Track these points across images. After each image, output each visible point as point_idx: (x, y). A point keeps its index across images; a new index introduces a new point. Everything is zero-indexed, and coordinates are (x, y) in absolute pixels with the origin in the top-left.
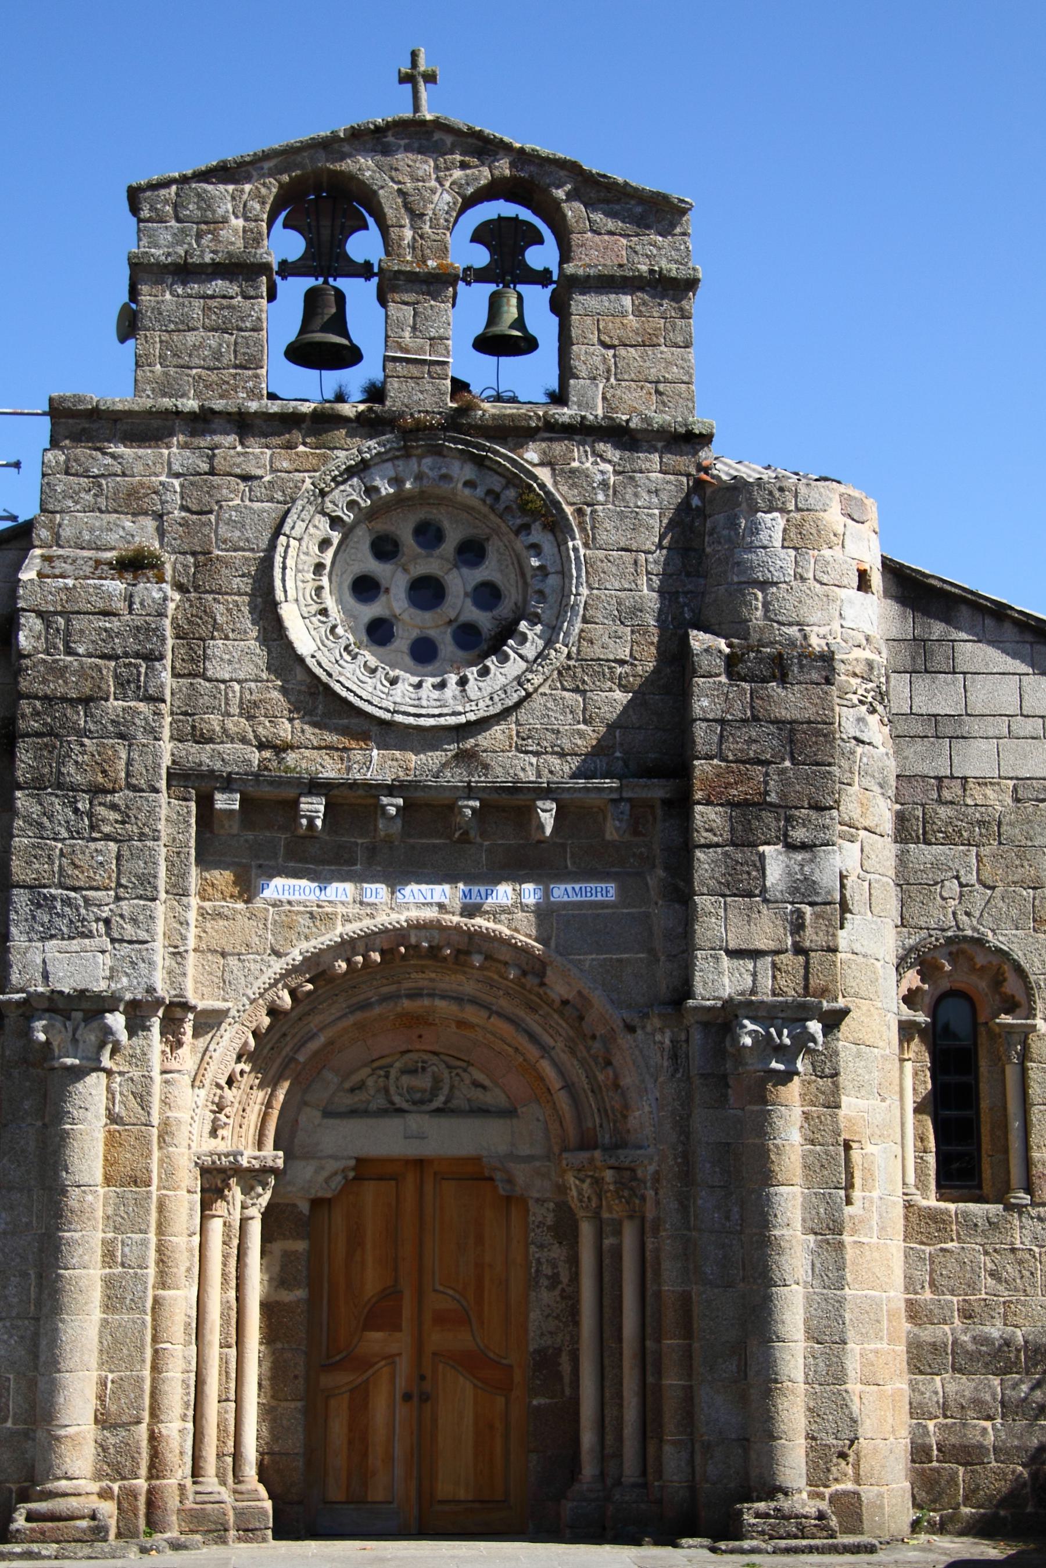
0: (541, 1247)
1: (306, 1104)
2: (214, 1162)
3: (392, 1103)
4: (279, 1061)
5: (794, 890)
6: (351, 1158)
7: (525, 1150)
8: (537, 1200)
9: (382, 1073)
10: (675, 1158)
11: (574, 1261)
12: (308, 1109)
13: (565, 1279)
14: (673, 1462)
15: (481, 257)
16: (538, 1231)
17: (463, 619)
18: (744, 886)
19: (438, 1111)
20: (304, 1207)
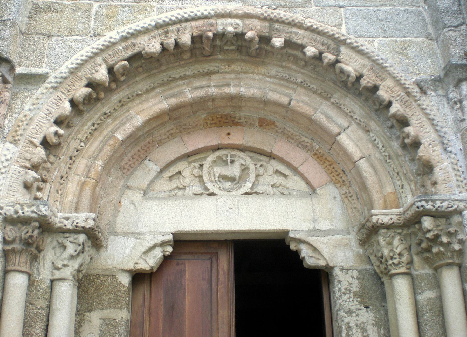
0: (350, 312)
1: (128, 187)
2: (16, 212)
3: (207, 189)
4: (101, 138)
6: (166, 234)
7: (325, 225)
8: (342, 269)
9: (197, 165)
12: (129, 193)
16: (345, 297)
19: (246, 194)
20: (125, 280)
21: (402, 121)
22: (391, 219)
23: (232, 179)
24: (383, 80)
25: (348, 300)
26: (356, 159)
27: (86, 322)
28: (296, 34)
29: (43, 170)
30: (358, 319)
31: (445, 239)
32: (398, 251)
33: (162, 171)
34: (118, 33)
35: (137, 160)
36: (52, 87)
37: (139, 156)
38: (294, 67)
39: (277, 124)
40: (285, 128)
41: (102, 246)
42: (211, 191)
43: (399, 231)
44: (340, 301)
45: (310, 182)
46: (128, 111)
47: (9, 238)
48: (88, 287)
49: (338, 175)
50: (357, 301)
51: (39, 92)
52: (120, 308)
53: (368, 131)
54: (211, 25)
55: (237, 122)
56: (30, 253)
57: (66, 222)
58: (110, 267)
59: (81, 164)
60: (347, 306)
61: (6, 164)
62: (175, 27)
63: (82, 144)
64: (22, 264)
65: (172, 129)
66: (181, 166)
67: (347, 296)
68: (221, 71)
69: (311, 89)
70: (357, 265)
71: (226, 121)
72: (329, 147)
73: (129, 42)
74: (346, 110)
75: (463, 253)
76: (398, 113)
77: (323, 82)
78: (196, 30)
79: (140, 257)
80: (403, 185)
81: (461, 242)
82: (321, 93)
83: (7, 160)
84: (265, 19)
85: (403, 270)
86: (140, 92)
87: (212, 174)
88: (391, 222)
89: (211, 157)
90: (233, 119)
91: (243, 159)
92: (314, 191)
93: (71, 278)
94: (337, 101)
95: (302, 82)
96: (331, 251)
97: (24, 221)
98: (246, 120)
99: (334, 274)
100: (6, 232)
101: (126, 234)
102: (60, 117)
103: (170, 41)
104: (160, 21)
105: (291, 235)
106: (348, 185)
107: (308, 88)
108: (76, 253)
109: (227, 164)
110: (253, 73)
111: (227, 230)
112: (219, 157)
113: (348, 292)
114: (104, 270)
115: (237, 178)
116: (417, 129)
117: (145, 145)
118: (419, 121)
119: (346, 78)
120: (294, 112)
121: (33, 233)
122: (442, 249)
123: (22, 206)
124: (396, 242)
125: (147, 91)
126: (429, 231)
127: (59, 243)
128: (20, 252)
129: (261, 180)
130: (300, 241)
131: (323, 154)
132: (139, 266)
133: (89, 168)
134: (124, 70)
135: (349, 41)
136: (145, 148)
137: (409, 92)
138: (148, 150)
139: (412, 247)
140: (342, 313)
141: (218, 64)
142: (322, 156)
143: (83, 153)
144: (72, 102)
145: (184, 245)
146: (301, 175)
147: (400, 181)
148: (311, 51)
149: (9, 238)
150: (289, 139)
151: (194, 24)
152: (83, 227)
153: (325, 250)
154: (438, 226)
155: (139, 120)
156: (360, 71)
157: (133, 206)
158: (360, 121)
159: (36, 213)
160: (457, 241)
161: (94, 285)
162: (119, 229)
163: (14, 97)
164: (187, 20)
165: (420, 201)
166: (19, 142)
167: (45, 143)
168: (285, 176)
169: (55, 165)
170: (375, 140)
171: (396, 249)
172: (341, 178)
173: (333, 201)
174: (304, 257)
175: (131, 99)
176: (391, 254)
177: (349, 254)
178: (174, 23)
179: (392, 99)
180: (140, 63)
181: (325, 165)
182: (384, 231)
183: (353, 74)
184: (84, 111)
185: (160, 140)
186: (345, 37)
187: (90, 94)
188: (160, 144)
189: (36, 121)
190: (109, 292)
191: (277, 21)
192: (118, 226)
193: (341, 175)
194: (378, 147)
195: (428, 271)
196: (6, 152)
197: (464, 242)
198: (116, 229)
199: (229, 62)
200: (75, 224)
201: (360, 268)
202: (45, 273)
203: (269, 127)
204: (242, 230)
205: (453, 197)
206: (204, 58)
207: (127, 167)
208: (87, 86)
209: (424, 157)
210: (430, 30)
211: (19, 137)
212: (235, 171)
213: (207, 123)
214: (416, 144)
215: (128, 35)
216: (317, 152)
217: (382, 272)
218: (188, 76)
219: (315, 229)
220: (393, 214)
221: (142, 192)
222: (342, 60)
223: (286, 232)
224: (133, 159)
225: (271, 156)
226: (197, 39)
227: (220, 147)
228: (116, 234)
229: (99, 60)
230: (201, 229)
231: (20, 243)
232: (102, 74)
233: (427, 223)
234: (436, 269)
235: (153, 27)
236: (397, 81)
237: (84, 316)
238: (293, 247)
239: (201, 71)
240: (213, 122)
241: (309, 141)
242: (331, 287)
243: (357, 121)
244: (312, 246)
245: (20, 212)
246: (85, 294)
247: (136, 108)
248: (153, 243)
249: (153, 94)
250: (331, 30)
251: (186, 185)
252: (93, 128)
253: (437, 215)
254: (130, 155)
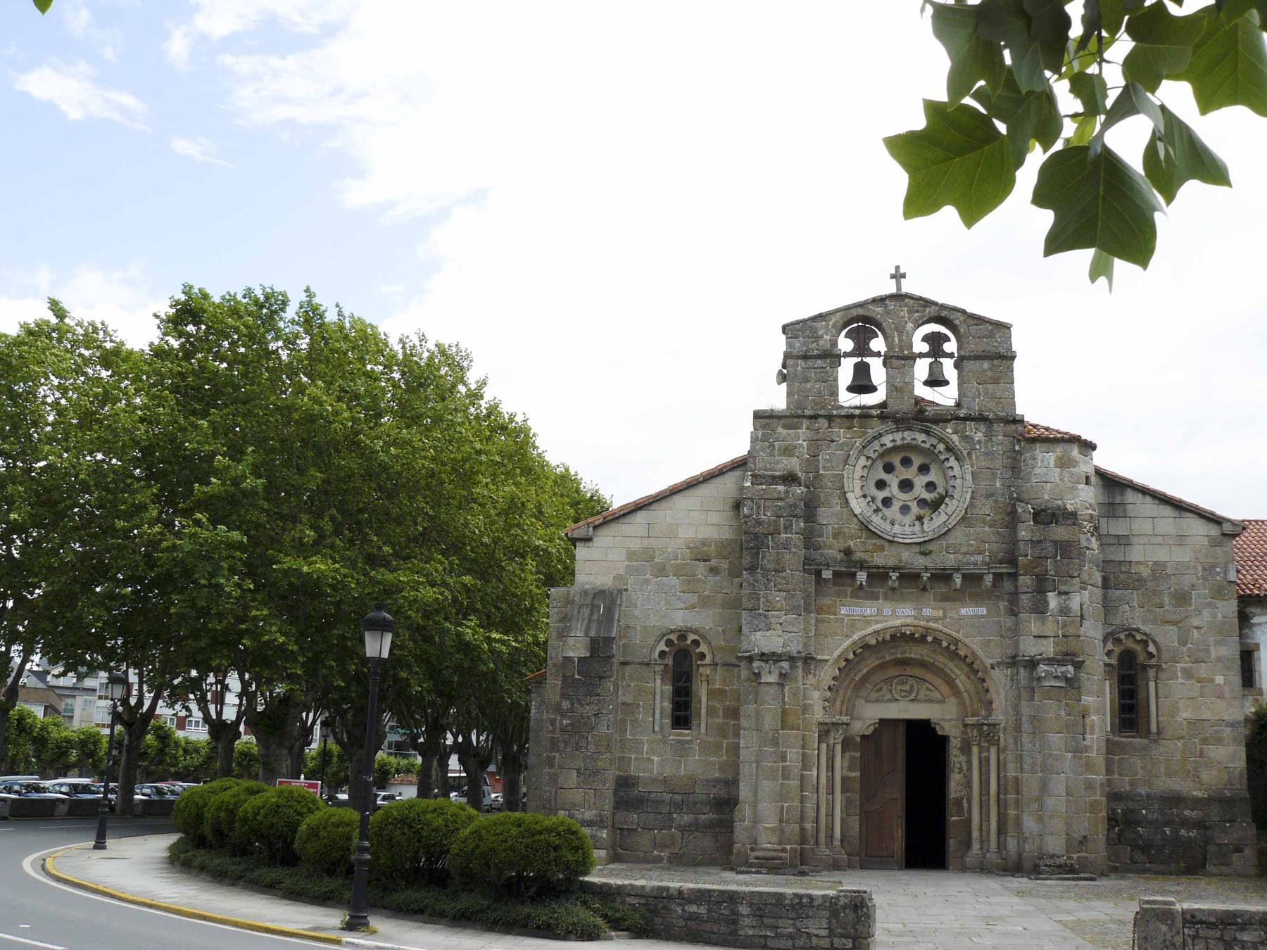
5: (1061, 611)
11: (969, 762)
13: (965, 768)
14: (1012, 844)
15: (925, 348)
17: (922, 496)
18: (1040, 609)
20: (858, 739)
48: (847, 744)
59: (841, 692)
91: (912, 681)
103: (880, 639)
145: (883, 722)
148: (945, 644)
155: (865, 671)
180: (866, 647)
199: (907, 642)
226: (893, 637)
232: (851, 656)
233: (985, 728)
250: (954, 634)
253: (988, 725)
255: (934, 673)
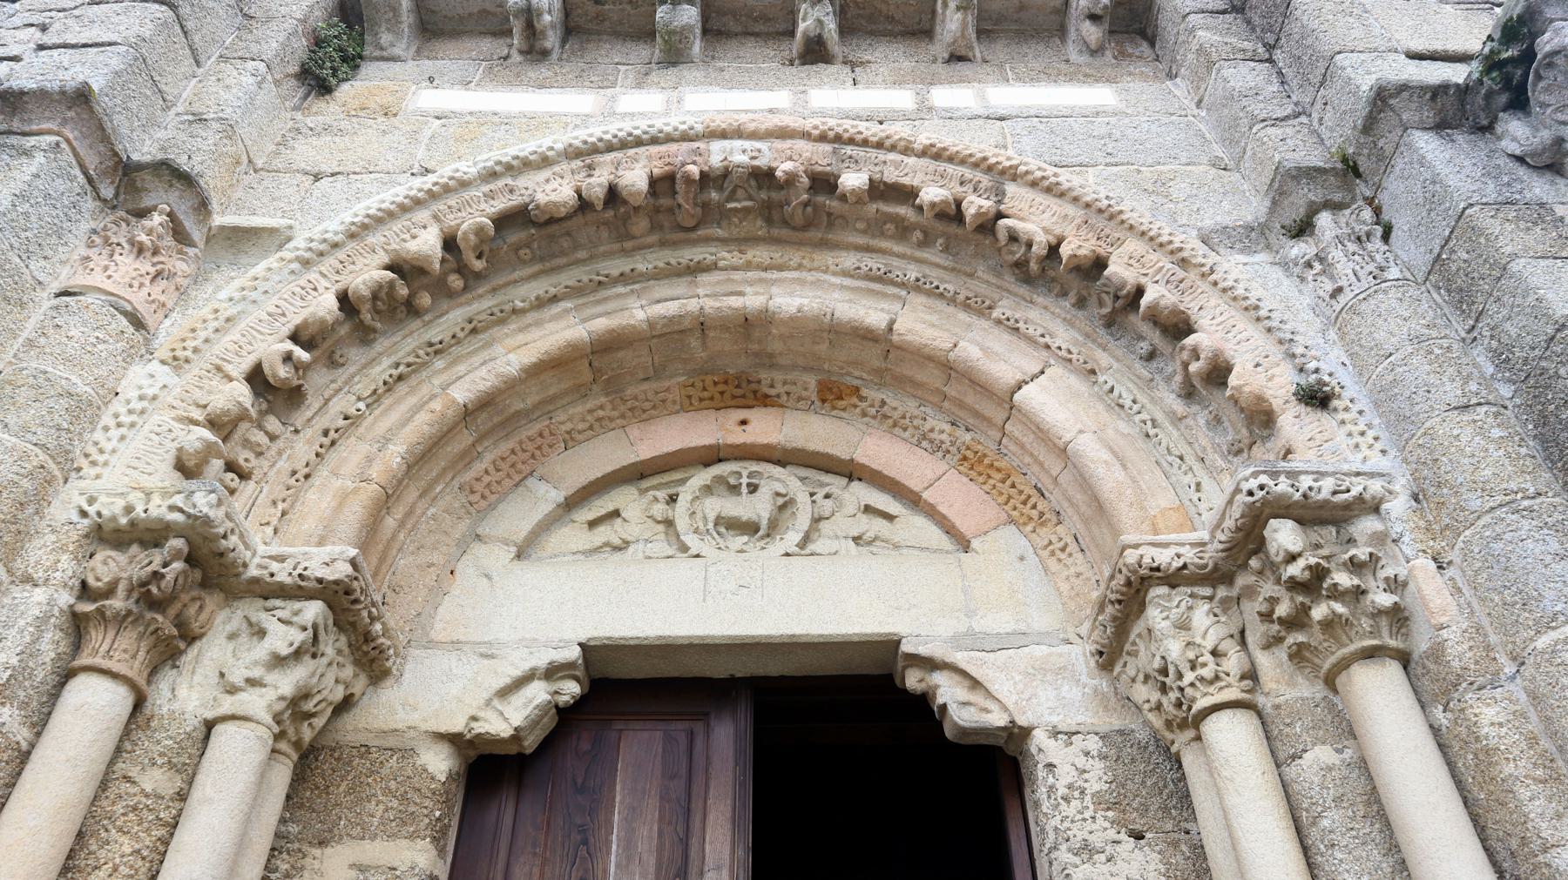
0: (1087, 850)
2: (129, 509)
4: (412, 400)
6: (565, 644)
7: (997, 622)
8: (1055, 733)
9: (662, 494)
10: (1481, 432)
12: (478, 549)
16: (1071, 810)
20: (439, 763)
21: (1176, 325)
22: (1179, 556)
23: (749, 528)
24: (1119, 242)
25: (1079, 817)
26: (1067, 437)
27: (306, 874)
28: (897, 165)
29: (244, 447)
30: (1114, 869)
31: (1343, 579)
32: (1209, 644)
33: (573, 503)
34: (475, 164)
35: (508, 476)
36: (298, 259)
37: (513, 466)
38: (898, 248)
39: (864, 392)
40: (883, 403)
41: (386, 673)
42: (693, 551)
43: (1207, 591)
44: (1055, 822)
45: (954, 527)
46: (488, 345)
47: (98, 579)
49: (1024, 503)
50: (1106, 818)
51: (263, 265)
52: (412, 837)
53: (1093, 372)
54: (697, 152)
55: (767, 396)
56: (152, 628)
57: (275, 566)
58: (400, 726)
59: (352, 452)
60: (1078, 833)
61: (138, 406)
62: (609, 157)
63: (362, 405)
64: (117, 655)
65: (601, 407)
66: (626, 499)
67: (1074, 803)
68: (721, 264)
69: (942, 294)
70: (1095, 721)
71: (739, 392)
72: (999, 435)
73: (500, 183)
74: (1031, 331)
75: (1407, 619)
76: (1163, 303)
77: (971, 276)
78: (659, 163)
79: (488, 703)
80: (1198, 485)
81: (1395, 585)
82: (968, 298)
83: (141, 398)
84: (823, 138)
85: (1233, 694)
86: (519, 304)
87: (699, 515)
88: (1177, 564)
89: (702, 477)
90: (754, 386)
92: (964, 544)
93: (268, 719)
94: (1009, 313)
95: (918, 280)
96: (1020, 686)
97: (147, 535)
98: (787, 388)
99: (1034, 750)
100: (92, 563)
101: (456, 645)
102: (305, 324)
104: (577, 143)
105: (906, 647)
106: (1054, 519)
107: (936, 294)
108: (291, 650)
109: (740, 494)
110: (799, 267)
111: (730, 637)
112: (720, 480)
113: (1076, 794)
114: (384, 733)
115: (764, 523)
116: (1218, 335)
117: (530, 439)
118: (1220, 319)
119: (1023, 249)
120: (903, 348)
121: (165, 565)
122: (1339, 608)
123: (148, 495)
124: (1201, 616)
125: (541, 303)
126: (1292, 558)
127: (250, 624)
128: (121, 621)
129: (824, 526)
130: (931, 664)
131: (985, 455)
132: (479, 728)
133: (369, 460)
134: (482, 241)
135: (1022, 168)
136: (530, 446)
137: (1183, 260)
138: (538, 453)
139: (1247, 633)
140: (1063, 855)
141: (714, 250)
142: (980, 461)
143: (361, 430)
144: (344, 299)
146: (931, 513)
147: (1190, 475)
149: (98, 579)
150: (897, 430)
151: (654, 149)
152: (320, 581)
153: (1001, 686)
154: (1318, 546)
156: (1058, 231)
157: (485, 580)
158: (1070, 352)
159: (181, 510)
160: (1382, 585)
161: (348, 772)
162: (439, 632)
163: (198, 279)
164: (639, 143)
165: (1255, 475)
166: (186, 366)
167: (256, 377)
168: (890, 517)
169: (280, 443)
170: (1112, 390)
171: (1204, 637)
172: (1034, 507)
173: (1017, 565)
174: (944, 707)
175: (501, 318)
176: (1191, 655)
177: (1072, 693)
178: (610, 148)
179: (1143, 280)
181: (991, 482)
182: (1163, 590)
183: (1041, 240)
184: (375, 331)
185: (568, 433)
186: (1014, 162)
187: (391, 284)
188: (570, 444)
189: (243, 325)
190: (387, 791)
191: (851, 141)
192: (438, 626)
193: (1033, 501)
194: (1122, 407)
195: (1306, 690)
196: (145, 382)
197: (1405, 584)
198: (433, 635)
199: (744, 242)
200: (299, 571)
201: (1104, 729)
202: (186, 695)
203: (841, 403)
204: (771, 637)
205: (1346, 467)
206: (682, 235)
207: (479, 487)
208: (388, 268)
209: (1246, 389)
210: (1218, 151)
211: (188, 353)
212: (758, 507)
213: (689, 397)
214: (1218, 373)
215: (498, 168)
216: (969, 454)
217: (1169, 724)
218: (641, 275)
219: (970, 633)
220: (1183, 545)
221: (514, 549)
222: (1010, 212)
223: (893, 644)
224: (498, 470)
225: (851, 472)
226: (662, 184)
227: (721, 455)
228: (432, 644)
229: (423, 215)
230: (660, 633)
231: (128, 598)
232: (426, 243)
233: (1284, 535)
234: (1330, 681)
235: (559, 155)
236: (1152, 239)
237: (304, 856)
238: (913, 680)
239: (673, 262)
240: (706, 394)
241: (947, 427)
242: (1027, 791)
243: (1063, 353)
244: (964, 674)
245: (139, 509)
246: (319, 797)
247: (510, 342)
248: (526, 666)
249: (556, 309)
251: (629, 539)
252: (395, 372)
253: (1311, 514)
254: (489, 457)
255: (894, 424)
